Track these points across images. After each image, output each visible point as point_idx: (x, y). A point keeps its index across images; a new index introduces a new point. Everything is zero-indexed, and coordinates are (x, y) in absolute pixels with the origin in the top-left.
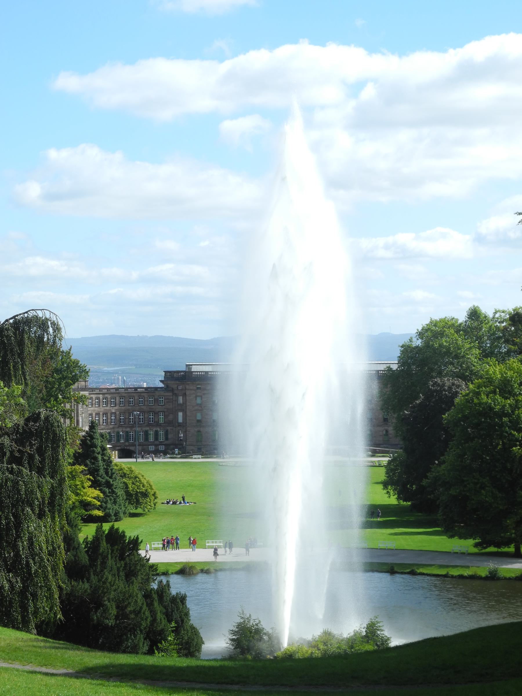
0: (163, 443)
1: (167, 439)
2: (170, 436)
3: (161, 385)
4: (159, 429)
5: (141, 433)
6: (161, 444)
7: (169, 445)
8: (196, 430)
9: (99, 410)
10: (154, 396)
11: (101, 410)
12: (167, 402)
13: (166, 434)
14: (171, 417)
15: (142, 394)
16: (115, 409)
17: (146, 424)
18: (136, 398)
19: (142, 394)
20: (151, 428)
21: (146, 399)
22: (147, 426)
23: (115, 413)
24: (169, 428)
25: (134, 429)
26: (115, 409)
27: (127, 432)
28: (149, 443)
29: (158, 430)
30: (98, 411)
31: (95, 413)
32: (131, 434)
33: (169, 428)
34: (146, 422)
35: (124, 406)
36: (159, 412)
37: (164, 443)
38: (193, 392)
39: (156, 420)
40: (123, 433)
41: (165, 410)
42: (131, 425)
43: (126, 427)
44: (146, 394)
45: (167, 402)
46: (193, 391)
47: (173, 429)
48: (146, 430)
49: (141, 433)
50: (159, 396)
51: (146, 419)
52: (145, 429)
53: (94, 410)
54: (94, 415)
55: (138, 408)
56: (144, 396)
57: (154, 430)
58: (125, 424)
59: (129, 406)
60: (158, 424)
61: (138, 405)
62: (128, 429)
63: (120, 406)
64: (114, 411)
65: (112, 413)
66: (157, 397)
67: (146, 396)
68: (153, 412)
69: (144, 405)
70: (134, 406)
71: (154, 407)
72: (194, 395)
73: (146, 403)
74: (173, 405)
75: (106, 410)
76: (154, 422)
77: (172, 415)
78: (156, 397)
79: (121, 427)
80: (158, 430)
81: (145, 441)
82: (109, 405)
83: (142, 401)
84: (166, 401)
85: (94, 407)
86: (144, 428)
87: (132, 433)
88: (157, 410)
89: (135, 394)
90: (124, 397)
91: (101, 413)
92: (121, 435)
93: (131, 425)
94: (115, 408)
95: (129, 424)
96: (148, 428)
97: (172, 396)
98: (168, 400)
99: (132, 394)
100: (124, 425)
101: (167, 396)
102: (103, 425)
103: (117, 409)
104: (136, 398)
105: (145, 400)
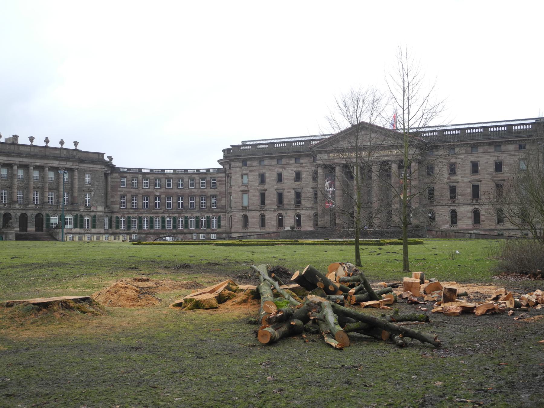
0: (215, 231)
1: (219, 226)
2: (223, 223)
3: (220, 167)
4: (211, 216)
5: (192, 220)
6: (213, 232)
7: (222, 233)
8: (242, 214)
9: (137, 192)
10: (206, 178)
11: (140, 192)
12: (220, 184)
13: (219, 221)
14: (223, 202)
15: (193, 176)
16: (159, 192)
17: (197, 210)
18: (186, 180)
19: (193, 176)
20: (203, 214)
21: (197, 181)
22: (198, 212)
23: (159, 196)
24: (221, 214)
25: (182, 215)
26: (159, 192)
27: (174, 218)
28: (200, 231)
29: (209, 216)
30: (135, 193)
31: (130, 195)
32: (181, 220)
33: (221, 214)
34: (197, 207)
35: (172, 189)
36: (211, 195)
37: (217, 231)
38: (238, 169)
39: (208, 204)
40: (170, 219)
41: (218, 193)
42: (179, 210)
43: (173, 213)
44: (197, 176)
45: (220, 184)
46: (239, 168)
47: (226, 215)
48: (197, 216)
49: (192, 220)
50: (211, 178)
51: (197, 204)
52: (195, 215)
53: (129, 192)
54: (129, 196)
55: (188, 191)
56: (195, 178)
57: (206, 216)
58: (172, 209)
59: (177, 189)
60: (210, 210)
61: (189, 187)
62: (176, 215)
63: (166, 189)
64: (158, 194)
65: (156, 196)
66: (209, 179)
67: (197, 178)
68: (206, 195)
69: (195, 188)
70: (184, 189)
71: (205, 190)
72: (240, 173)
73: (197, 185)
74: (226, 187)
75: (147, 192)
76: (206, 208)
77: (225, 199)
78: (208, 179)
79: (167, 212)
80: (209, 216)
81: (195, 229)
82: (152, 187)
83: (193, 183)
84: (218, 183)
85: (129, 188)
86: (195, 214)
87: (182, 219)
88: (210, 194)
89: (184, 176)
90: (172, 178)
91: (140, 196)
92: (168, 221)
93: (179, 210)
94: (160, 190)
95: (177, 209)
96: (199, 215)
97: (225, 177)
98: (220, 182)
99: (181, 176)
100: (171, 210)
101: (220, 177)
102: (131, 209)
103: (162, 192)
104: (186, 180)
105: (196, 182)
